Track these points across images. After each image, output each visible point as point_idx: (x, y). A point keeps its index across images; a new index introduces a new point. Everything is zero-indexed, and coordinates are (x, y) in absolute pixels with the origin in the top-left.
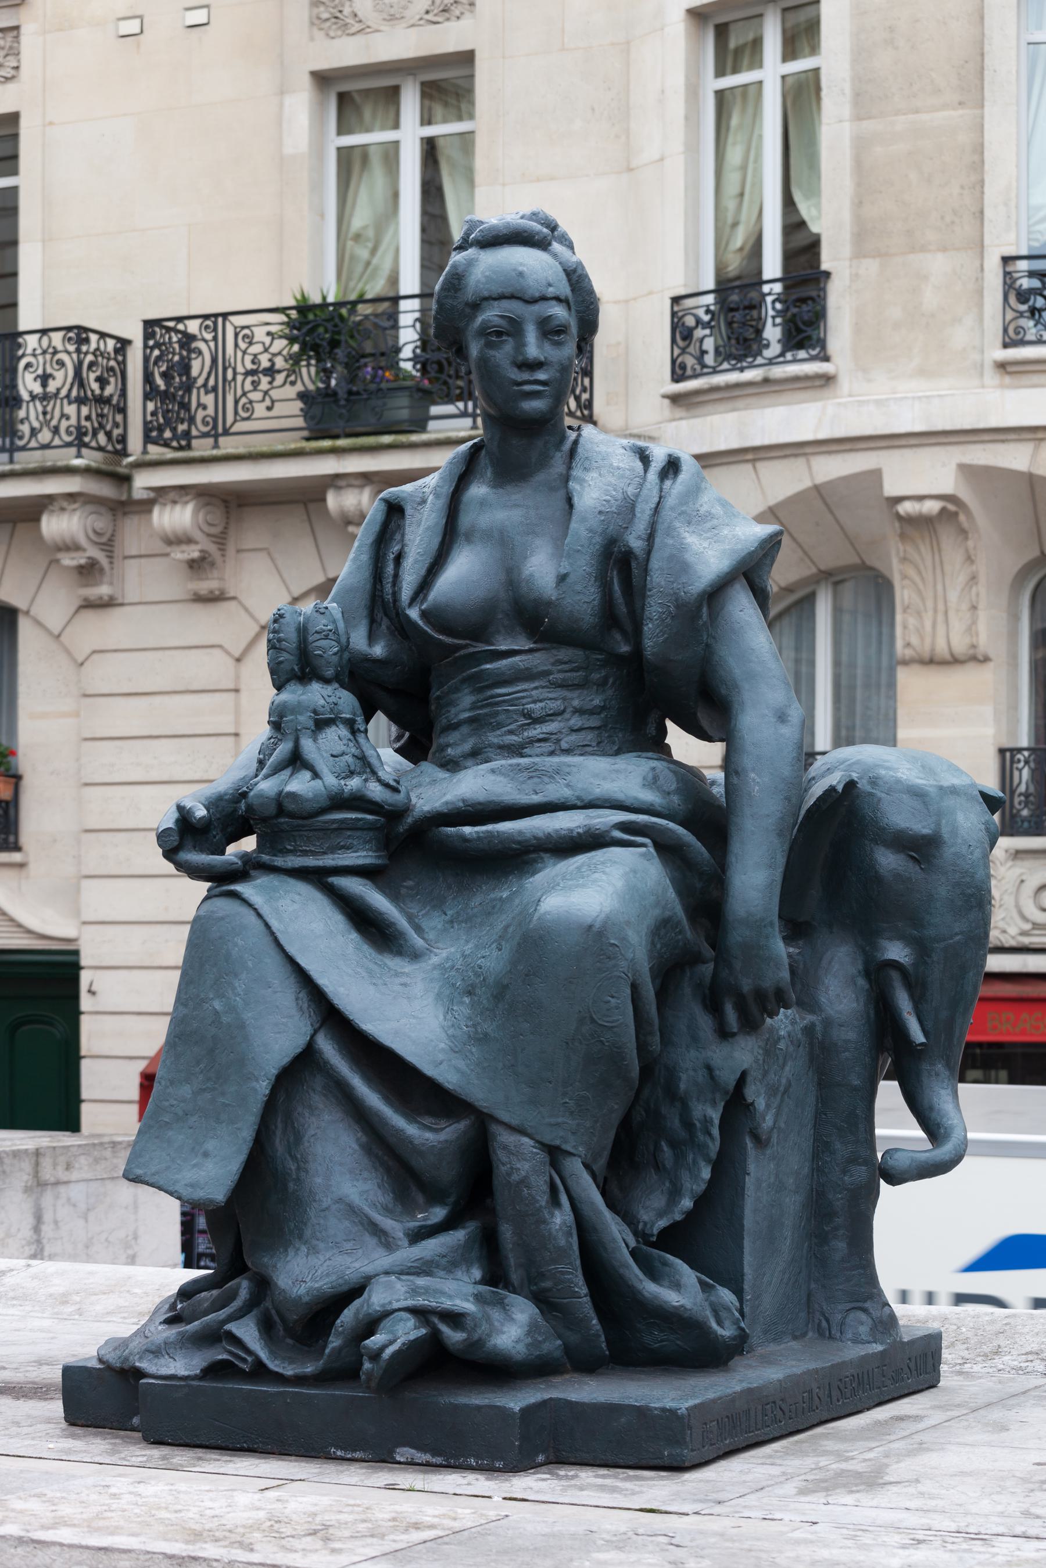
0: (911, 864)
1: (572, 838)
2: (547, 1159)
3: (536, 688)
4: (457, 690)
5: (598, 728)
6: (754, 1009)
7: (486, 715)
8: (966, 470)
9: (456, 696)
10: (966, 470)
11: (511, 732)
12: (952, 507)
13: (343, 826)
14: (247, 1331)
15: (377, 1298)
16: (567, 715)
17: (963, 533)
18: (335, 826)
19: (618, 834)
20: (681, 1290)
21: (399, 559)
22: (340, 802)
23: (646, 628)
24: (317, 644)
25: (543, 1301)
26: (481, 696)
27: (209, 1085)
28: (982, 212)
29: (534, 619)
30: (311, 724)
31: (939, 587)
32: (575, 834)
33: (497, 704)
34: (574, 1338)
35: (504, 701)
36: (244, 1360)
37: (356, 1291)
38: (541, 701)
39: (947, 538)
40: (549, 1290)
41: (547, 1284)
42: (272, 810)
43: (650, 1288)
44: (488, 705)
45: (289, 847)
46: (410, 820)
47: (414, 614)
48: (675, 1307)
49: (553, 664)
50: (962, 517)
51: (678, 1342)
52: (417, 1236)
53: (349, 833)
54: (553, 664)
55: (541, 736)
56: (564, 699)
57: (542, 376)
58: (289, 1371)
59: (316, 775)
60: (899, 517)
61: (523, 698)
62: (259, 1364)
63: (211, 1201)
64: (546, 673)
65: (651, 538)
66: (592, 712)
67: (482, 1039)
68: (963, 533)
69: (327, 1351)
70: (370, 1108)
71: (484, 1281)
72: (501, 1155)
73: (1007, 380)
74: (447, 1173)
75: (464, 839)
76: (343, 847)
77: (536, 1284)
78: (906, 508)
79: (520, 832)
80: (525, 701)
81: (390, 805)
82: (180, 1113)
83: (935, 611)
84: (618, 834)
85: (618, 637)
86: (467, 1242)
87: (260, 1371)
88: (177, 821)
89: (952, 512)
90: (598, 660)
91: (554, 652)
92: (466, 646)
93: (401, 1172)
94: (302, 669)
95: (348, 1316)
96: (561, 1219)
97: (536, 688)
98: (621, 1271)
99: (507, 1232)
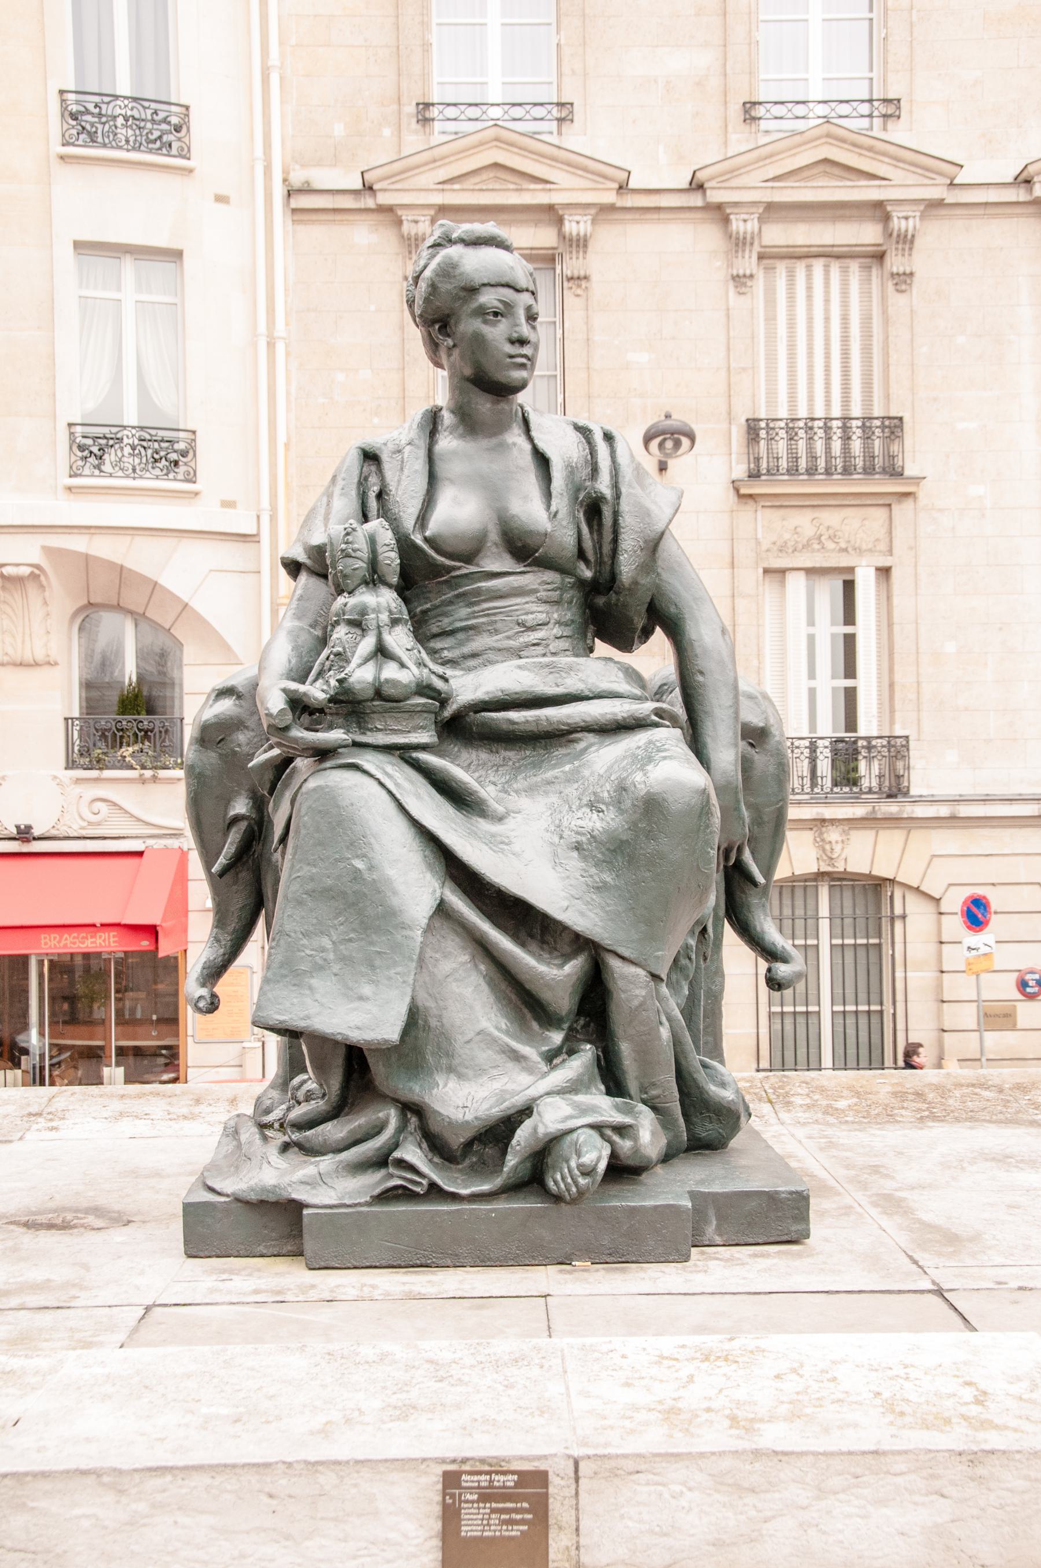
0: (749, 748)
3: (527, 603)
4: (450, 603)
7: (483, 623)
8: (47, 550)
9: (450, 608)
10: (49, 551)
11: (509, 638)
12: (37, 572)
14: (413, 1153)
16: (551, 626)
17: (42, 587)
18: (419, 709)
23: (621, 558)
24: (386, 554)
26: (476, 608)
27: (352, 935)
28: (54, 395)
31: (27, 619)
32: (619, 718)
33: (494, 614)
37: (526, 1111)
38: (532, 613)
39: (32, 589)
40: (658, 1097)
41: (654, 1092)
42: (370, 693)
44: (485, 615)
45: (379, 727)
49: (539, 584)
50: (42, 578)
53: (425, 715)
54: (539, 584)
55: (535, 641)
56: (548, 613)
58: (465, 1192)
60: (3, 576)
61: (517, 610)
62: (433, 1186)
63: (386, 1041)
64: (535, 591)
67: (600, 888)
68: (42, 587)
70: (504, 950)
72: (621, 983)
73: (72, 496)
75: (512, 722)
76: (422, 727)
77: (646, 1093)
79: (569, 716)
80: (518, 613)
82: (321, 962)
83: (24, 634)
84: (654, 718)
87: (435, 1191)
89: (36, 576)
91: (540, 574)
92: (459, 568)
93: (525, 1002)
95: (522, 1135)
97: (527, 603)
98: (695, 1076)
99: (625, 1049)
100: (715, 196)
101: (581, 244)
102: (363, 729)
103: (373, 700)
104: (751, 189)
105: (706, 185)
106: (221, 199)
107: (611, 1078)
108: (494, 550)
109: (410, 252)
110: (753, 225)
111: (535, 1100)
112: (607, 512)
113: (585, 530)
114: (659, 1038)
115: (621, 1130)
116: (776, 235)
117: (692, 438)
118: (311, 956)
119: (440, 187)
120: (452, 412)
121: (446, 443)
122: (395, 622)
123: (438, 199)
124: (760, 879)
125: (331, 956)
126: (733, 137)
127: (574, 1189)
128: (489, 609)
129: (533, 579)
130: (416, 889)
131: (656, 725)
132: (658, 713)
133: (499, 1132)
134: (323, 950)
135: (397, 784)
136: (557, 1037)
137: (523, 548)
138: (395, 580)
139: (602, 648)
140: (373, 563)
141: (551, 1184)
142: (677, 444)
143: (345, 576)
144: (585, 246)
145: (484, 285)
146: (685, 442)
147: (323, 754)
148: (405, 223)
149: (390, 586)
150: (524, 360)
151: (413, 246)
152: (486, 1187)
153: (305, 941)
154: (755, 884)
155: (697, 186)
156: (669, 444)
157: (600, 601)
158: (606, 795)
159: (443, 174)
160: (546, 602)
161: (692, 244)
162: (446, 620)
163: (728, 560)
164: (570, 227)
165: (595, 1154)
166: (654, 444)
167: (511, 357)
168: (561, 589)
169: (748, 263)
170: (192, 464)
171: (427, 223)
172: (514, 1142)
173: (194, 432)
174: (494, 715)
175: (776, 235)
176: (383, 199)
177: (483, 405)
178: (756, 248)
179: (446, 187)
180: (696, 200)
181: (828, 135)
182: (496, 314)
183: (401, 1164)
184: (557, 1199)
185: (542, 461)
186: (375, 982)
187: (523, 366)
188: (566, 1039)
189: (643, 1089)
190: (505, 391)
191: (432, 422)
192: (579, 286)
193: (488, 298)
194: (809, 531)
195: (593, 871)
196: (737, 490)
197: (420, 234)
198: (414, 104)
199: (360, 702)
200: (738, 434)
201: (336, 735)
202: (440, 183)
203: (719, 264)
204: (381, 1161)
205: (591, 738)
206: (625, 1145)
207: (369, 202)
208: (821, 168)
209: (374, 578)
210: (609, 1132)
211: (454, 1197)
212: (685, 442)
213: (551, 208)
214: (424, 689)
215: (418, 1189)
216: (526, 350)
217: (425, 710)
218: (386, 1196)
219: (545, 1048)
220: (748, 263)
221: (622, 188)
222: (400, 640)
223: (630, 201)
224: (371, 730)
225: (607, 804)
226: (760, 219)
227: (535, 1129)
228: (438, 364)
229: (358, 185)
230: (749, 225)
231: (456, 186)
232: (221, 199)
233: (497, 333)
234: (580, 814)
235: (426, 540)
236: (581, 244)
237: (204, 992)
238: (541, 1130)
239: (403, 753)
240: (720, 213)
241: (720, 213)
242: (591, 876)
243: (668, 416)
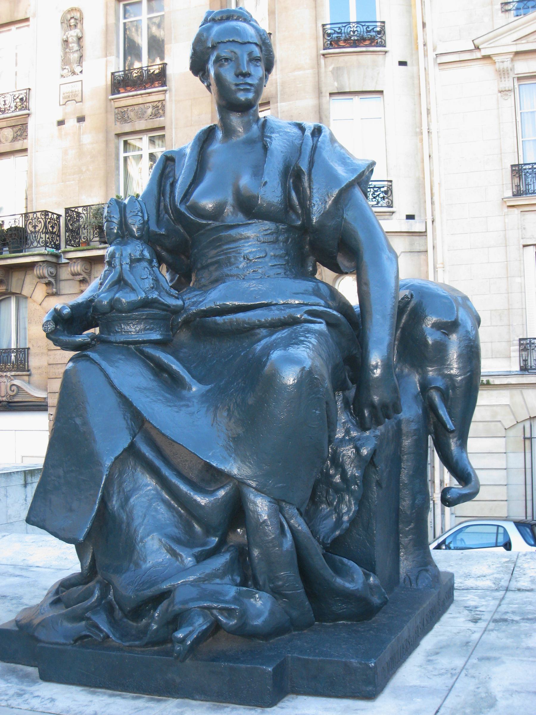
1: (280, 320)
2: (278, 508)
5: (285, 265)
6: (380, 414)
13: (149, 317)
16: (267, 259)
19: (305, 316)
20: (355, 580)
21: (173, 185)
22: (146, 304)
25: (276, 593)
26: (219, 250)
27: (73, 468)
30: (128, 261)
33: (230, 253)
34: (295, 614)
35: (233, 251)
40: (282, 586)
43: (339, 581)
44: (224, 254)
47: (183, 209)
48: (352, 590)
51: (353, 609)
52: (200, 558)
57: (249, 80)
59: (133, 290)
65: (311, 163)
66: (280, 257)
71: (244, 583)
77: (273, 583)
81: (174, 306)
84: (305, 316)
85: (294, 217)
86: (231, 558)
90: (283, 228)
94: (123, 233)
96: (288, 542)
106: (403, 63)
109: (501, 78)
118: (53, 480)
119: (515, 43)
123: (514, 49)
128: (227, 249)
134: (59, 477)
137: (248, 207)
140: (123, 224)
145: (219, 43)
148: (497, 63)
149: (138, 238)
150: (249, 87)
151: (502, 74)
167: (237, 85)
168: (277, 232)
170: (390, 198)
171: (509, 62)
173: (391, 181)
176: (484, 52)
179: (517, 42)
189: (271, 580)
190: (246, 108)
197: (505, 68)
198: (499, 4)
202: (515, 41)
207: (478, 55)
224: (113, 333)
229: (472, 47)
231: (523, 42)
232: (403, 63)
242: (231, 430)
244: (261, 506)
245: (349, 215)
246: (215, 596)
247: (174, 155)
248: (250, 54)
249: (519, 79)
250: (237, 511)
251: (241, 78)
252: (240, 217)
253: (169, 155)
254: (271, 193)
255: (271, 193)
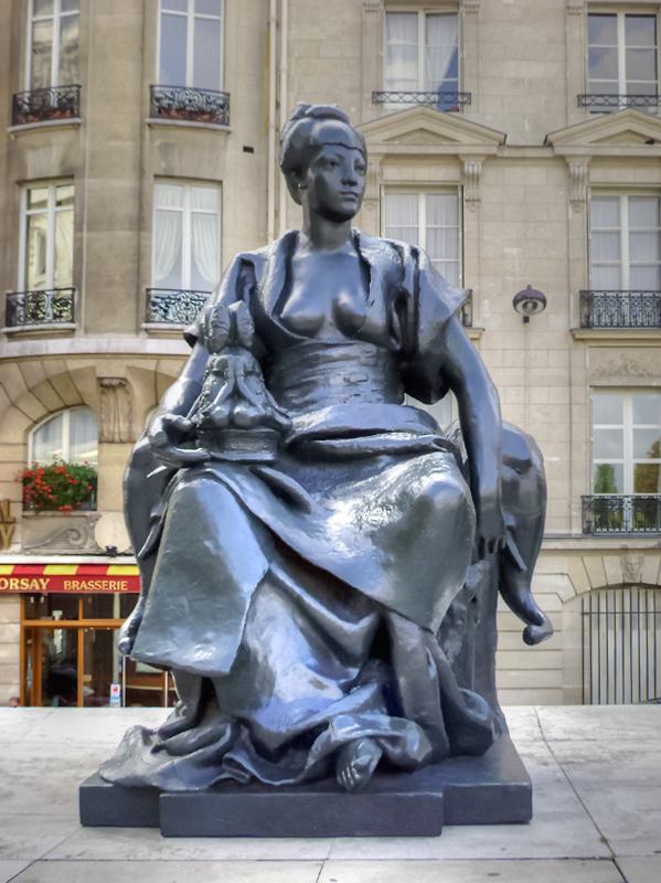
8: (130, 368)
15: (339, 733)
17: (127, 392)
19: (434, 446)
29: (350, 327)
36: (244, 777)
37: (324, 725)
39: (120, 393)
41: (423, 713)
42: (226, 422)
46: (293, 437)
52: (347, 689)
60: (102, 385)
62: (253, 778)
68: (127, 392)
69: (307, 767)
70: (315, 610)
72: (399, 633)
74: (358, 647)
75: (332, 447)
78: (106, 382)
82: (180, 615)
84: (434, 446)
88: (164, 428)
93: (327, 647)
100: (559, 151)
101: (475, 179)
102: (222, 450)
103: (228, 427)
104: (583, 146)
105: (555, 144)
107: (391, 701)
108: (330, 328)
110: (583, 170)
111: (330, 718)
112: (411, 302)
113: (395, 316)
114: (428, 674)
115: (394, 740)
116: (599, 175)
117: (544, 301)
120: (306, 233)
121: (301, 254)
122: (248, 374)
123: (384, 150)
124: (523, 566)
125: (187, 609)
126: (571, 116)
127: (352, 782)
129: (359, 350)
130: (247, 561)
131: (437, 450)
132: (438, 442)
133: (305, 738)
135: (242, 488)
136: (354, 672)
138: (249, 344)
139: (409, 400)
140: (234, 331)
141: (339, 778)
142: (535, 306)
143: (214, 341)
144: (478, 179)
146: (540, 304)
147: (194, 465)
149: (248, 349)
152: (291, 781)
153: (168, 600)
154: (519, 570)
155: (548, 144)
156: (530, 305)
157: (404, 365)
158: (393, 498)
159: (387, 135)
160: (365, 365)
161: (540, 178)
162: (295, 377)
163: (567, 380)
164: (469, 169)
165: (368, 757)
166: (520, 305)
167: (343, 193)
168: (378, 356)
169: (581, 192)
172: (314, 748)
174: (321, 442)
175: (599, 175)
177: (327, 228)
178: (586, 183)
180: (547, 153)
181: (630, 116)
182: (333, 164)
183: (231, 762)
184: (342, 789)
185: (365, 266)
186: (216, 630)
187: (353, 200)
188: (360, 675)
189: (416, 711)
190: (341, 218)
191: (290, 243)
192: (473, 205)
193: (328, 153)
194: (619, 363)
195: (381, 552)
196: (573, 336)
199: (219, 429)
200: (574, 300)
201: (200, 452)
203: (562, 193)
204: (217, 760)
205: (385, 459)
206: (395, 751)
208: (626, 136)
209: (234, 342)
210: (382, 741)
211: (270, 788)
212: (540, 304)
213: (456, 157)
214: (266, 421)
215: (243, 781)
216: (354, 189)
217: (268, 436)
218: (219, 786)
219: (343, 681)
220: (581, 192)
221: (502, 144)
222: (254, 387)
223: (506, 153)
225: (393, 504)
226: (588, 166)
227: (329, 736)
228: (298, 201)
230: (581, 169)
233: (333, 178)
234: (375, 512)
235: (281, 320)
236: (475, 179)
237: (127, 639)
238: (333, 738)
239: (253, 469)
240: (562, 160)
241: (562, 160)
243: (529, 287)
244: (408, 636)
245: (451, 344)
246: (372, 725)
247: (252, 260)
248: (357, 161)
249: (387, 187)
250: (381, 645)
251: (348, 186)
252: (338, 336)
253: (245, 258)
254: (375, 314)
255: (375, 314)
